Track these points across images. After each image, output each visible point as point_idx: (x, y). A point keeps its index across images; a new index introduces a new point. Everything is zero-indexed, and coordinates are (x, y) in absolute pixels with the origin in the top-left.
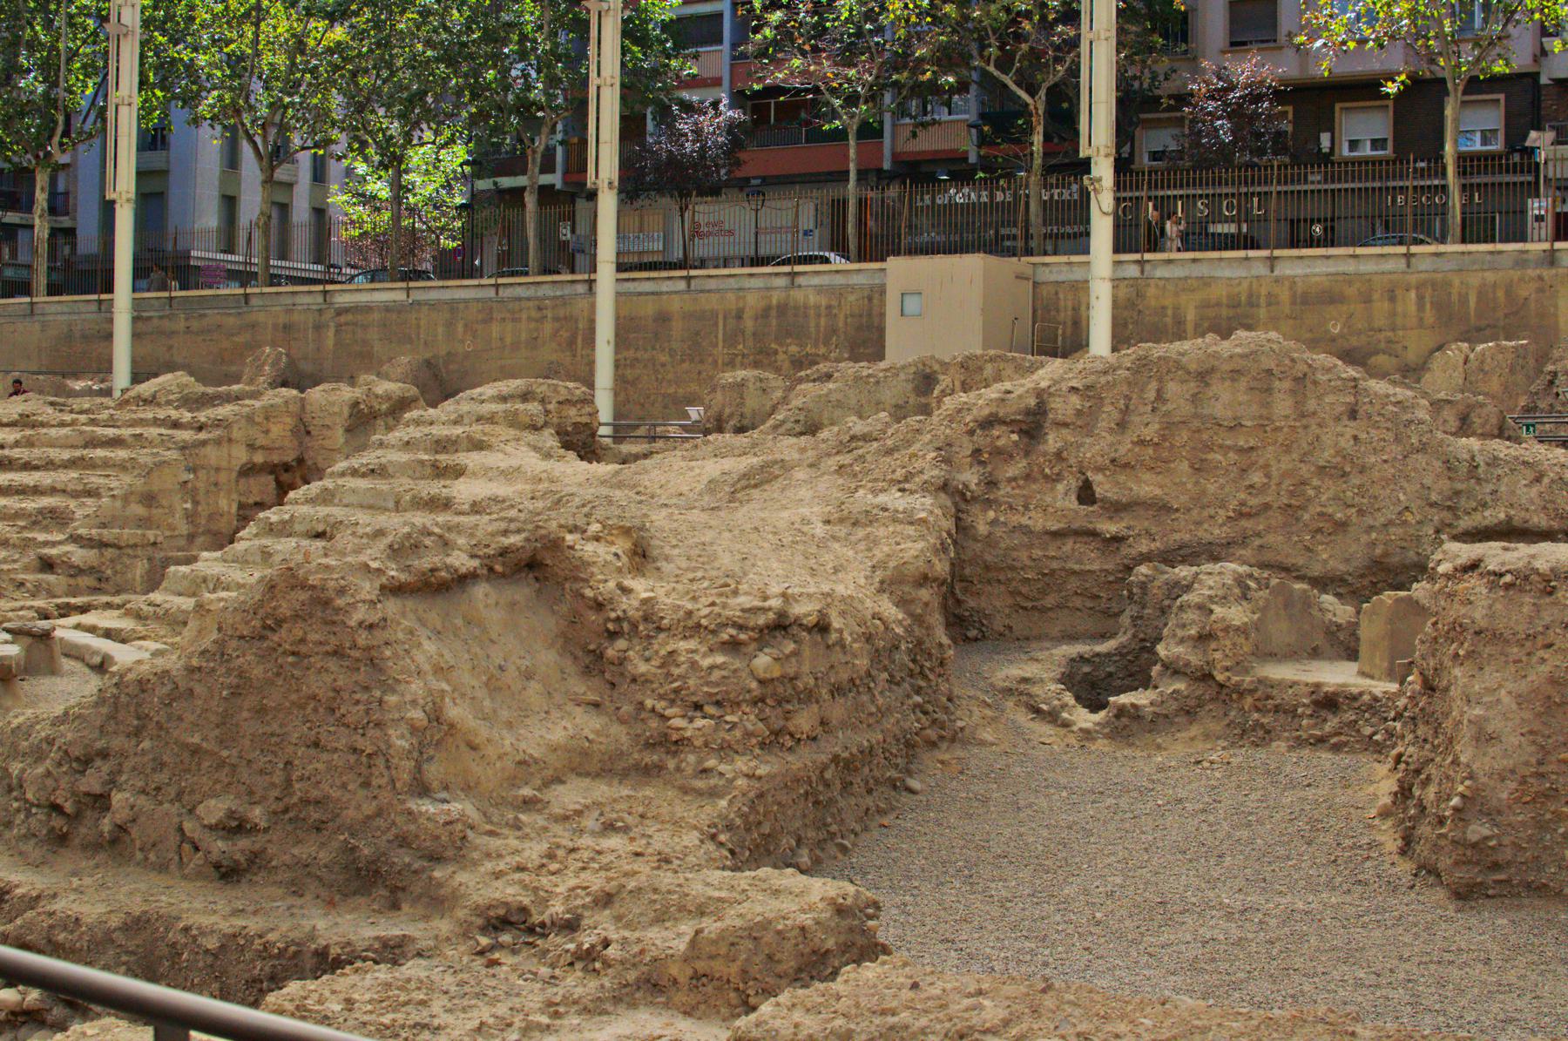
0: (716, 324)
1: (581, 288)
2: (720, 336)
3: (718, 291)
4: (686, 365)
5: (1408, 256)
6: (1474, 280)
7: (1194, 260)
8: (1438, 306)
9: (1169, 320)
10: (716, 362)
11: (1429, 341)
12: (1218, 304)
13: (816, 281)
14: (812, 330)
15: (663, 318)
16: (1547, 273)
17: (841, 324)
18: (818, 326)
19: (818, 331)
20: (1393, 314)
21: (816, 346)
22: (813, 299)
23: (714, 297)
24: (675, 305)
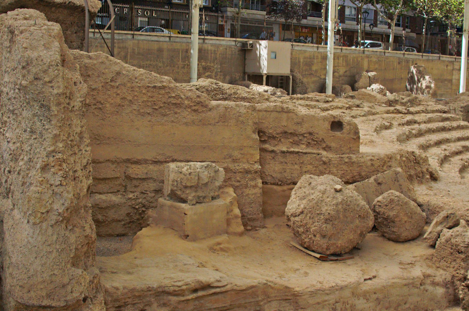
0: (179, 54)
1: (130, 37)
2: (180, 58)
3: (180, 42)
4: (168, 68)
5: (341, 49)
6: (352, 56)
7: (303, 46)
8: (346, 61)
9: (297, 61)
10: (178, 67)
11: (344, 70)
12: (307, 58)
13: (211, 42)
14: (210, 58)
15: (160, 50)
16: (363, 55)
17: (218, 57)
18: (211, 56)
19: (211, 59)
20: (338, 63)
21: (210, 63)
22: (210, 48)
23: (179, 44)
24: (165, 46)
